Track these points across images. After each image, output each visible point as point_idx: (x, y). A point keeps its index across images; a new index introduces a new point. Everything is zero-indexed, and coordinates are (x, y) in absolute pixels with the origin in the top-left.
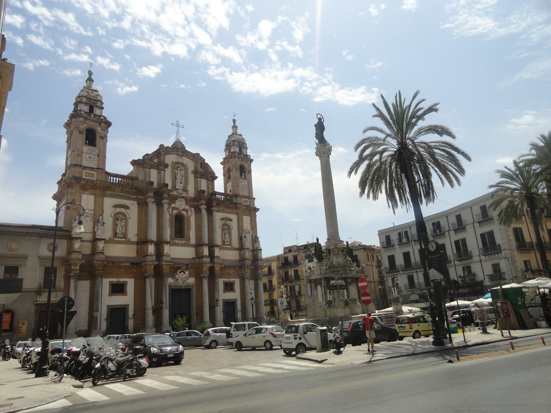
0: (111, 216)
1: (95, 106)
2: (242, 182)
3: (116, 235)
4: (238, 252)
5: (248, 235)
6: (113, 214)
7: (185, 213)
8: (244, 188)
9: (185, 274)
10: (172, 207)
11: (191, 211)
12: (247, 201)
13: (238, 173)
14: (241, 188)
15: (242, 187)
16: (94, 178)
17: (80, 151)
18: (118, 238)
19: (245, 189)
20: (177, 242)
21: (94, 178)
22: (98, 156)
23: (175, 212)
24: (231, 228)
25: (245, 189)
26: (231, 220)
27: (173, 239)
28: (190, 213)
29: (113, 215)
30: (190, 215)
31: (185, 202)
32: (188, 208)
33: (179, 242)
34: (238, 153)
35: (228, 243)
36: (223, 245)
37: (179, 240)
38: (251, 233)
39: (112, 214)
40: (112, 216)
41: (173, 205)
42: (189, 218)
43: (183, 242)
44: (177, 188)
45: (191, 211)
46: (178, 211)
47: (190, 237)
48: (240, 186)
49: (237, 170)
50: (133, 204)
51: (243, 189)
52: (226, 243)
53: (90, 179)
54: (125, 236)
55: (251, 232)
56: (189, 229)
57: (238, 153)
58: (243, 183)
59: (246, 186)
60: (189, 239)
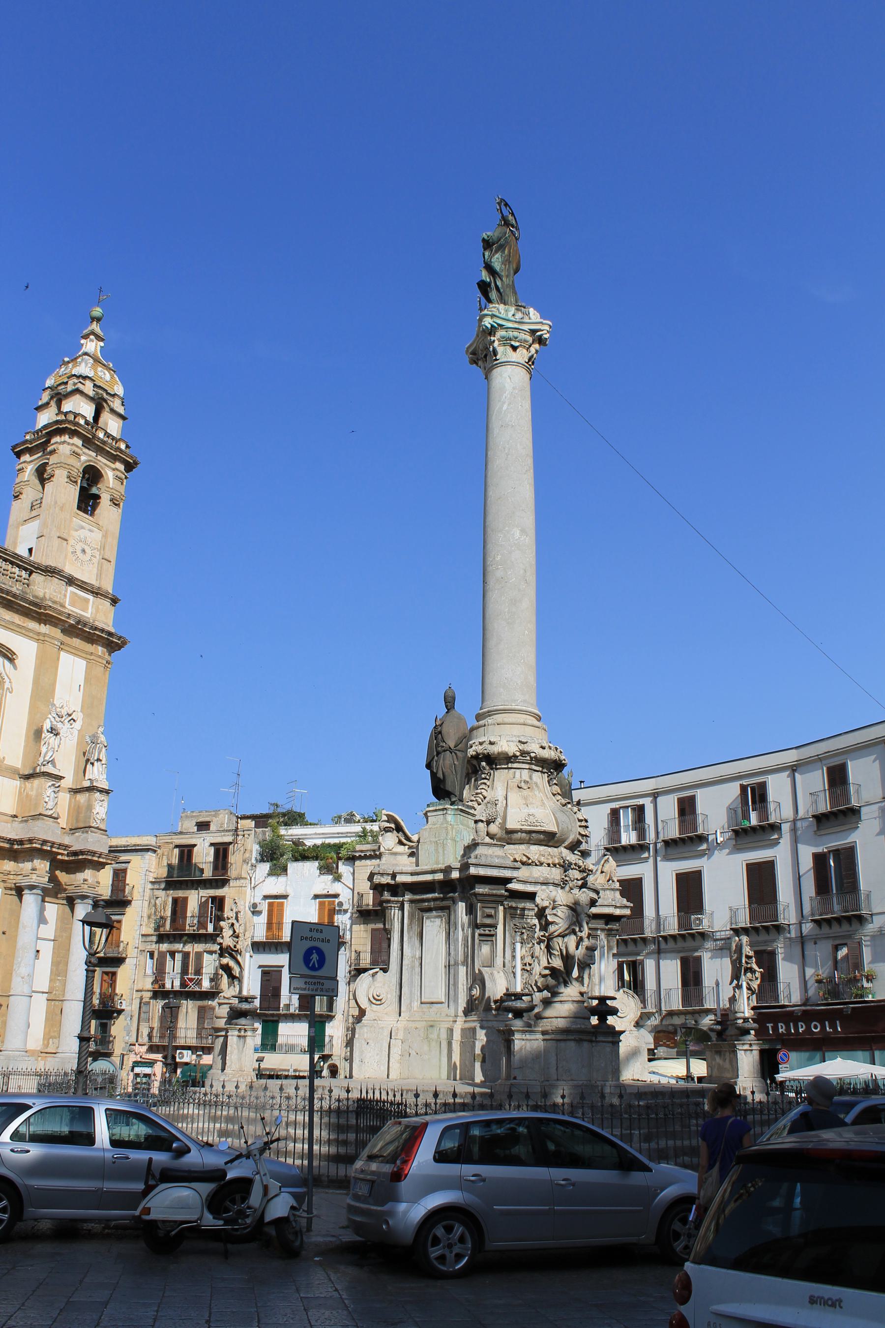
2: (82, 528)
4: (17, 783)
5: (67, 725)
8: (84, 551)
12: (87, 601)
13: (73, 493)
14: (71, 550)
24: (7, 685)
34: (87, 423)
38: (78, 725)
48: (71, 542)
49: (71, 480)
55: (79, 716)
57: (87, 423)
58: (82, 533)
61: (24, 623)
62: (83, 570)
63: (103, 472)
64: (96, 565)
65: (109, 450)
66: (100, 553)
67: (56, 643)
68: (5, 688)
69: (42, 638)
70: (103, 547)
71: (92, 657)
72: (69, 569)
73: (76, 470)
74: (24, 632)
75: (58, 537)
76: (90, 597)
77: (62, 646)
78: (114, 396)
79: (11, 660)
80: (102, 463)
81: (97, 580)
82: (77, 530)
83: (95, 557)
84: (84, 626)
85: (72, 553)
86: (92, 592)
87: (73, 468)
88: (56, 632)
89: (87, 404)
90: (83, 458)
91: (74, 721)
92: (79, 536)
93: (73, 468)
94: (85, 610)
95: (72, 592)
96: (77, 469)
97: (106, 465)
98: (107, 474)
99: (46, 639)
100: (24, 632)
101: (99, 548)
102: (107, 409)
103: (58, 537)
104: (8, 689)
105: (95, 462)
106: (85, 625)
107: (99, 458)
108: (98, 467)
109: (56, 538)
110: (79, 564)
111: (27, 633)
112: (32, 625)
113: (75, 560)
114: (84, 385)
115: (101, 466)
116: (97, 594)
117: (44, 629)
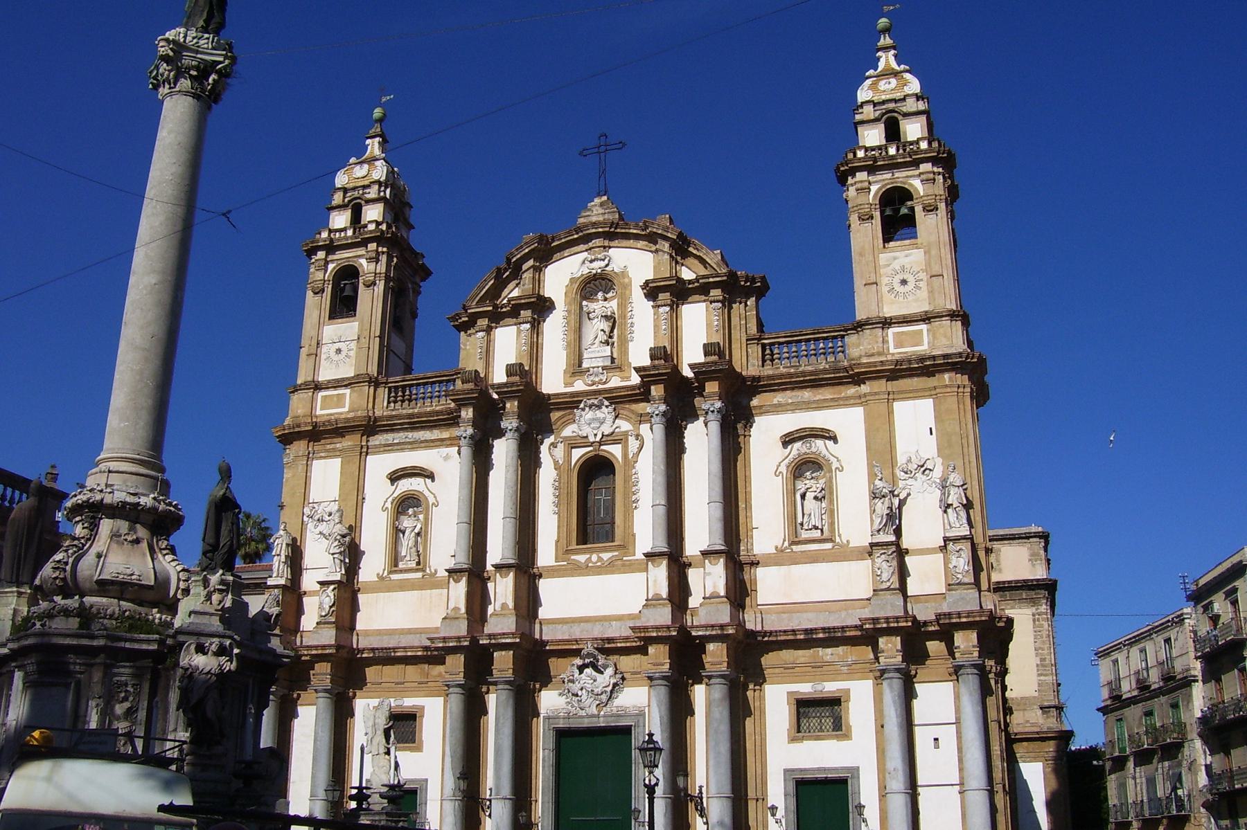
0: (384, 509)
1: (363, 202)
2: (895, 258)
3: (396, 566)
6: (390, 499)
7: (615, 451)
8: (904, 282)
9: (602, 673)
10: (566, 439)
11: (638, 436)
17: (314, 343)
18: (401, 571)
20: (582, 558)
23: (577, 454)
24: (835, 465)
25: (911, 286)
26: (828, 436)
27: (568, 552)
28: (633, 444)
29: (389, 505)
30: (636, 450)
31: (610, 409)
32: (624, 426)
33: (589, 560)
35: (817, 534)
36: (793, 543)
37: (591, 551)
39: (385, 502)
40: (387, 508)
41: (568, 431)
42: (630, 463)
43: (606, 556)
45: (638, 436)
46: (591, 448)
47: (634, 535)
48: (885, 280)
50: (447, 458)
51: (901, 289)
52: (805, 535)
53: (331, 415)
54: (421, 564)
56: (630, 506)
59: (916, 269)
60: (627, 546)
63: (906, 186)
65: (902, 160)
67: (882, 397)
68: (833, 468)
69: (863, 400)
70: (928, 264)
71: (938, 390)
72: (889, 311)
73: (867, 206)
74: (842, 403)
75: (865, 285)
76: (923, 327)
77: (891, 398)
78: (904, 99)
79: (834, 439)
80: (902, 177)
82: (889, 265)
83: (922, 280)
84: (910, 364)
86: (924, 320)
87: (862, 207)
88: (880, 385)
89: (873, 128)
90: (874, 188)
91: (930, 470)
92: (894, 270)
93: (862, 207)
95: (895, 334)
96: (868, 204)
97: (907, 177)
98: (911, 185)
99: (868, 398)
100: (842, 403)
101: (924, 268)
102: (900, 118)
103: (865, 285)
105: (892, 183)
106: (910, 361)
107: (897, 175)
108: (899, 185)
109: (862, 287)
111: (847, 403)
112: (852, 391)
113: (895, 297)
114: (862, 113)
115: (901, 182)
116: (929, 319)
117: (864, 388)
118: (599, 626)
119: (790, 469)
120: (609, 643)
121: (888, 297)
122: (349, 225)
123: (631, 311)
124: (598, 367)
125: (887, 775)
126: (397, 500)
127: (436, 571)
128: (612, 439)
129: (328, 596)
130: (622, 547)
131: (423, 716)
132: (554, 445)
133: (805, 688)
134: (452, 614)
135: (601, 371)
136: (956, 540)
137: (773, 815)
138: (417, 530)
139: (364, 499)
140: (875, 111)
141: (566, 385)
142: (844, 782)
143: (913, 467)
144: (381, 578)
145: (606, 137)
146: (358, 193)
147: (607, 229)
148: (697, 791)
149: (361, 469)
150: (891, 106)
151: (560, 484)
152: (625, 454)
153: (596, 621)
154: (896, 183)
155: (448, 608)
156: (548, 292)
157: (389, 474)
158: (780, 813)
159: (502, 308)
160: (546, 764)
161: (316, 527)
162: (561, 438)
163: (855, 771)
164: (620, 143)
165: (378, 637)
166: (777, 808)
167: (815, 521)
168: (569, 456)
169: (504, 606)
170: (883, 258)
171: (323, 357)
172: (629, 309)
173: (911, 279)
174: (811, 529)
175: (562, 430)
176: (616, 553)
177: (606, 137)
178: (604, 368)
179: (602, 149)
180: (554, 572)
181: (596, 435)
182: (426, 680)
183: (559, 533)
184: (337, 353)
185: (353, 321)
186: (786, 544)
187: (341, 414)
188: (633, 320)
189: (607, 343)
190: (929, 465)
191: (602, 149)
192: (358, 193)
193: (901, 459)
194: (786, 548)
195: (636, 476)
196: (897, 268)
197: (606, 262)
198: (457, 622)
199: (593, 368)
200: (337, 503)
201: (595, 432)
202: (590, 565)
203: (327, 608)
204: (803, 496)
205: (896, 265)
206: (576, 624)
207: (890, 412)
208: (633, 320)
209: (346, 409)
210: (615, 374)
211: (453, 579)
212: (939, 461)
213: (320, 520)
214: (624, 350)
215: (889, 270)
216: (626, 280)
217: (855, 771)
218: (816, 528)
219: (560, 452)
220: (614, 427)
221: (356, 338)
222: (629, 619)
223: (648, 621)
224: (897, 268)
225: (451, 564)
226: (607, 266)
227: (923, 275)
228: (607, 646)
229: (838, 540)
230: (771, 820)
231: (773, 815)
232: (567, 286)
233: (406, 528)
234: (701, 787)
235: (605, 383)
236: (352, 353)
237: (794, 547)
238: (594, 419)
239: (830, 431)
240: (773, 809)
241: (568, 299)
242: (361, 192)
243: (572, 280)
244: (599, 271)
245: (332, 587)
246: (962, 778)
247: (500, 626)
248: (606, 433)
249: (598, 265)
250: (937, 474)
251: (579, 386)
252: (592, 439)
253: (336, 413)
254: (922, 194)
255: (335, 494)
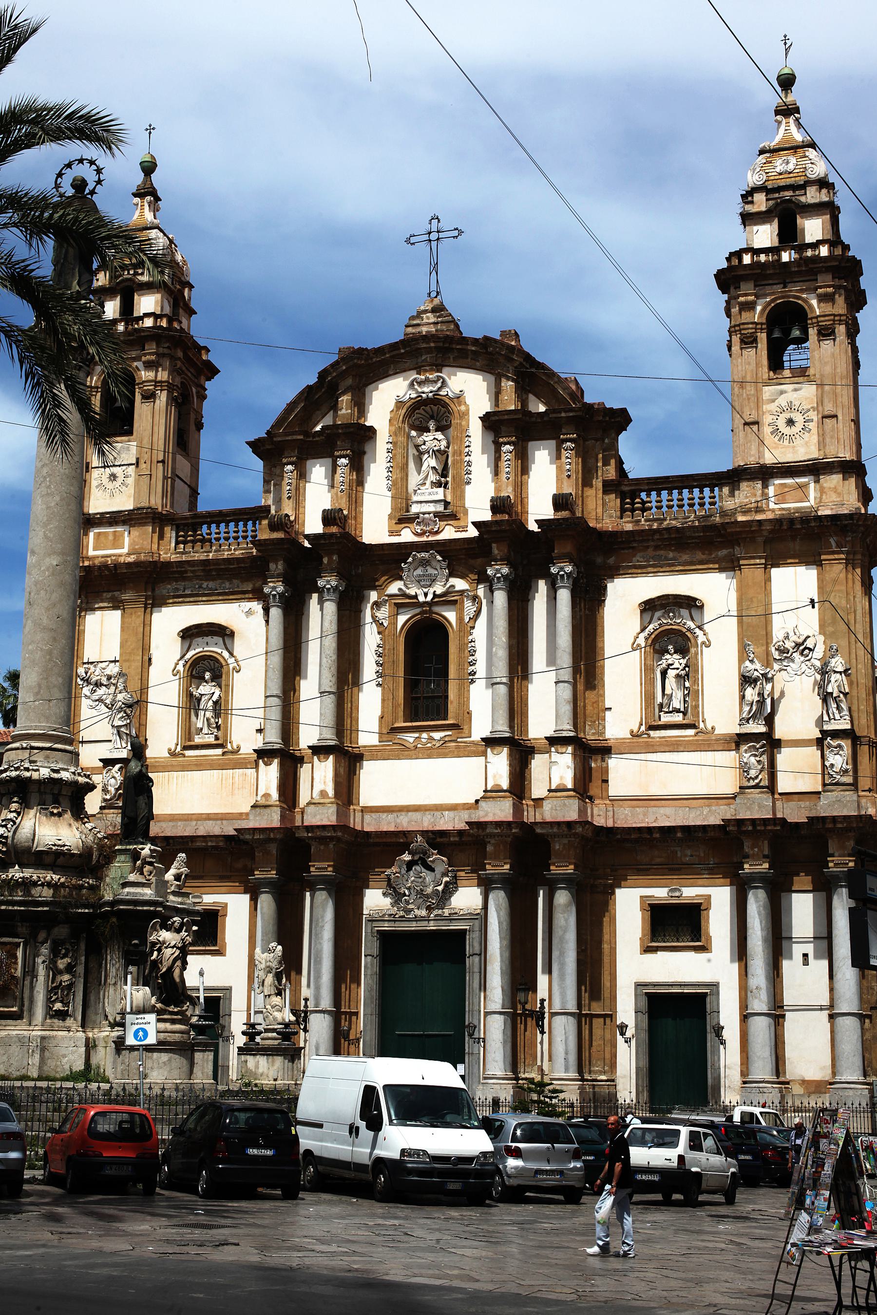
2: (782, 392)
8: (790, 422)
9: (433, 870)
11: (475, 598)
15: (781, 423)
16: (95, 549)
19: (799, 426)
20: (410, 738)
21: (95, 549)
22: (137, 464)
24: (701, 638)
25: (799, 426)
27: (394, 730)
28: (469, 608)
29: (180, 667)
35: (678, 718)
42: (466, 628)
44: (415, 509)
45: (475, 598)
48: (767, 419)
50: (249, 613)
51: (787, 430)
53: (107, 556)
59: (806, 407)
61: (711, 554)
62: (794, 447)
64: (814, 431)
66: (818, 412)
68: (699, 642)
70: (821, 402)
81: (819, 450)
82: (773, 401)
83: (812, 421)
85: (772, 433)
87: (746, 326)
91: (810, 650)
94: (806, 498)
101: (815, 405)
104: (703, 643)
110: (786, 443)
113: (779, 440)
118: (429, 817)
119: (650, 641)
120: (441, 837)
121: (769, 439)
122: (117, 316)
123: (469, 446)
124: (429, 513)
125: (749, 994)
126: (189, 663)
127: (239, 748)
128: (449, 599)
129: (114, 777)
130: (455, 727)
131: (226, 915)
132: (377, 605)
133: (660, 893)
134: (263, 802)
135: (433, 518)
136: (836, 734)
137: (623, 1034)
138: (215, 698)
139: (150, 659)
140: (767, 200)
141: (392, 533)
142: (701, 999)
143: (789, 645)
144: (173, 754)
145: (439, 221)
146: (129, 273)
147: (441, 344)
148: (539, 1005)
149: (147, 625)
150: (788, 194)
151: (384, 650)
152: (460, 619)
153: (426, 810)
154: (789, 297)
155: (257, 795)
156: (371, 421)
157: (181, 631)
158: (630, 1033)
159: (314, 437)
160: (369, 972)
161: (93, 692)
162: (386, 595)
163: (715, 986)
164: (456, 229)
165: (171, 824)
166: (627, 1026)
167: (677, 703)
168: (394, 617)
169: (323, 793)
170: (768, 391)
171: (94, 483)
172: (467, 444)
173: (798, 418)
174: (671, 712)
175: (387, 586)
176: (449, 733)
177: (439, 221)
178: (436, 514)
179: (434, 236)
180: (377, 754)
181: (426, 595)
182: (228, 874)
183: (383, 707)
184: (111, 480)
185: (129, 441)
186: (643, 728)
187: (120, 556)
188: (471, 458)
189: (438, 484)
190: (809, 643)
191: (434, 236)
192: (129, 273)
193: (777, 634)
194: (643, 733)
195: (473, 644)
196: (784, 404)
197: (439, 385)
198: (268, 810)
199: (424, 514)
200: (117, 664)
201: (425, 590)
202: (419, 746)
203: (113, 790)
204: (664, 674)
205: (782, 401)
206: (403, 813)
207: (768, 580)
208: (471, 458)
209: (125, 550)
210: (450, 522)
211: (263, 762)
212: (821, 638)
213: (98, 684)
214: (460, 495)
215: (773, 407)
216: (463, 408)
217: (715, 986)
218: (678, 711)
219: (383, 613)
220: (448, 586)
221: (134, 461)
222: (464, 809)
223: (486, 815)
224: (784, 404)
225: (258, 742)
226: (439, 389)
227: (813, 415)
228: (438, 840)
229: (702, 725)
230: (620, 1039)
231: (623, 1034)
232: (392, 411)
233: (202, 695)
234: (543, 1001)
235: (437, 533)
236: (130, 481)
237: (652, 733)
238: (424, 575)
239: (697, 599)
240: (623, 1028)
241: (393, 429)
242: (132, 272)
243: (399, 404)
244: (431, 395)
245: (118, 766)
246: (832, 999)
247: (318, 817)
248: (438, 592)
249: (427, 390)
250: (819, 653)
251: (407, 536)
252: (421, 599)
253: (114, 555)
254: (818, 314)
255: (115, 652)
